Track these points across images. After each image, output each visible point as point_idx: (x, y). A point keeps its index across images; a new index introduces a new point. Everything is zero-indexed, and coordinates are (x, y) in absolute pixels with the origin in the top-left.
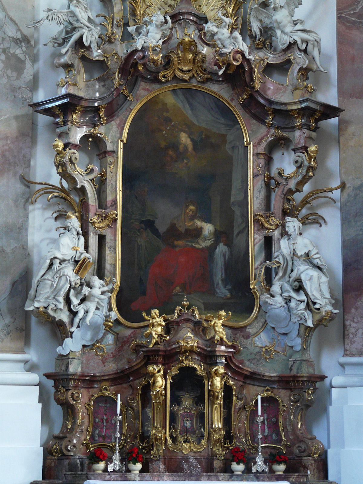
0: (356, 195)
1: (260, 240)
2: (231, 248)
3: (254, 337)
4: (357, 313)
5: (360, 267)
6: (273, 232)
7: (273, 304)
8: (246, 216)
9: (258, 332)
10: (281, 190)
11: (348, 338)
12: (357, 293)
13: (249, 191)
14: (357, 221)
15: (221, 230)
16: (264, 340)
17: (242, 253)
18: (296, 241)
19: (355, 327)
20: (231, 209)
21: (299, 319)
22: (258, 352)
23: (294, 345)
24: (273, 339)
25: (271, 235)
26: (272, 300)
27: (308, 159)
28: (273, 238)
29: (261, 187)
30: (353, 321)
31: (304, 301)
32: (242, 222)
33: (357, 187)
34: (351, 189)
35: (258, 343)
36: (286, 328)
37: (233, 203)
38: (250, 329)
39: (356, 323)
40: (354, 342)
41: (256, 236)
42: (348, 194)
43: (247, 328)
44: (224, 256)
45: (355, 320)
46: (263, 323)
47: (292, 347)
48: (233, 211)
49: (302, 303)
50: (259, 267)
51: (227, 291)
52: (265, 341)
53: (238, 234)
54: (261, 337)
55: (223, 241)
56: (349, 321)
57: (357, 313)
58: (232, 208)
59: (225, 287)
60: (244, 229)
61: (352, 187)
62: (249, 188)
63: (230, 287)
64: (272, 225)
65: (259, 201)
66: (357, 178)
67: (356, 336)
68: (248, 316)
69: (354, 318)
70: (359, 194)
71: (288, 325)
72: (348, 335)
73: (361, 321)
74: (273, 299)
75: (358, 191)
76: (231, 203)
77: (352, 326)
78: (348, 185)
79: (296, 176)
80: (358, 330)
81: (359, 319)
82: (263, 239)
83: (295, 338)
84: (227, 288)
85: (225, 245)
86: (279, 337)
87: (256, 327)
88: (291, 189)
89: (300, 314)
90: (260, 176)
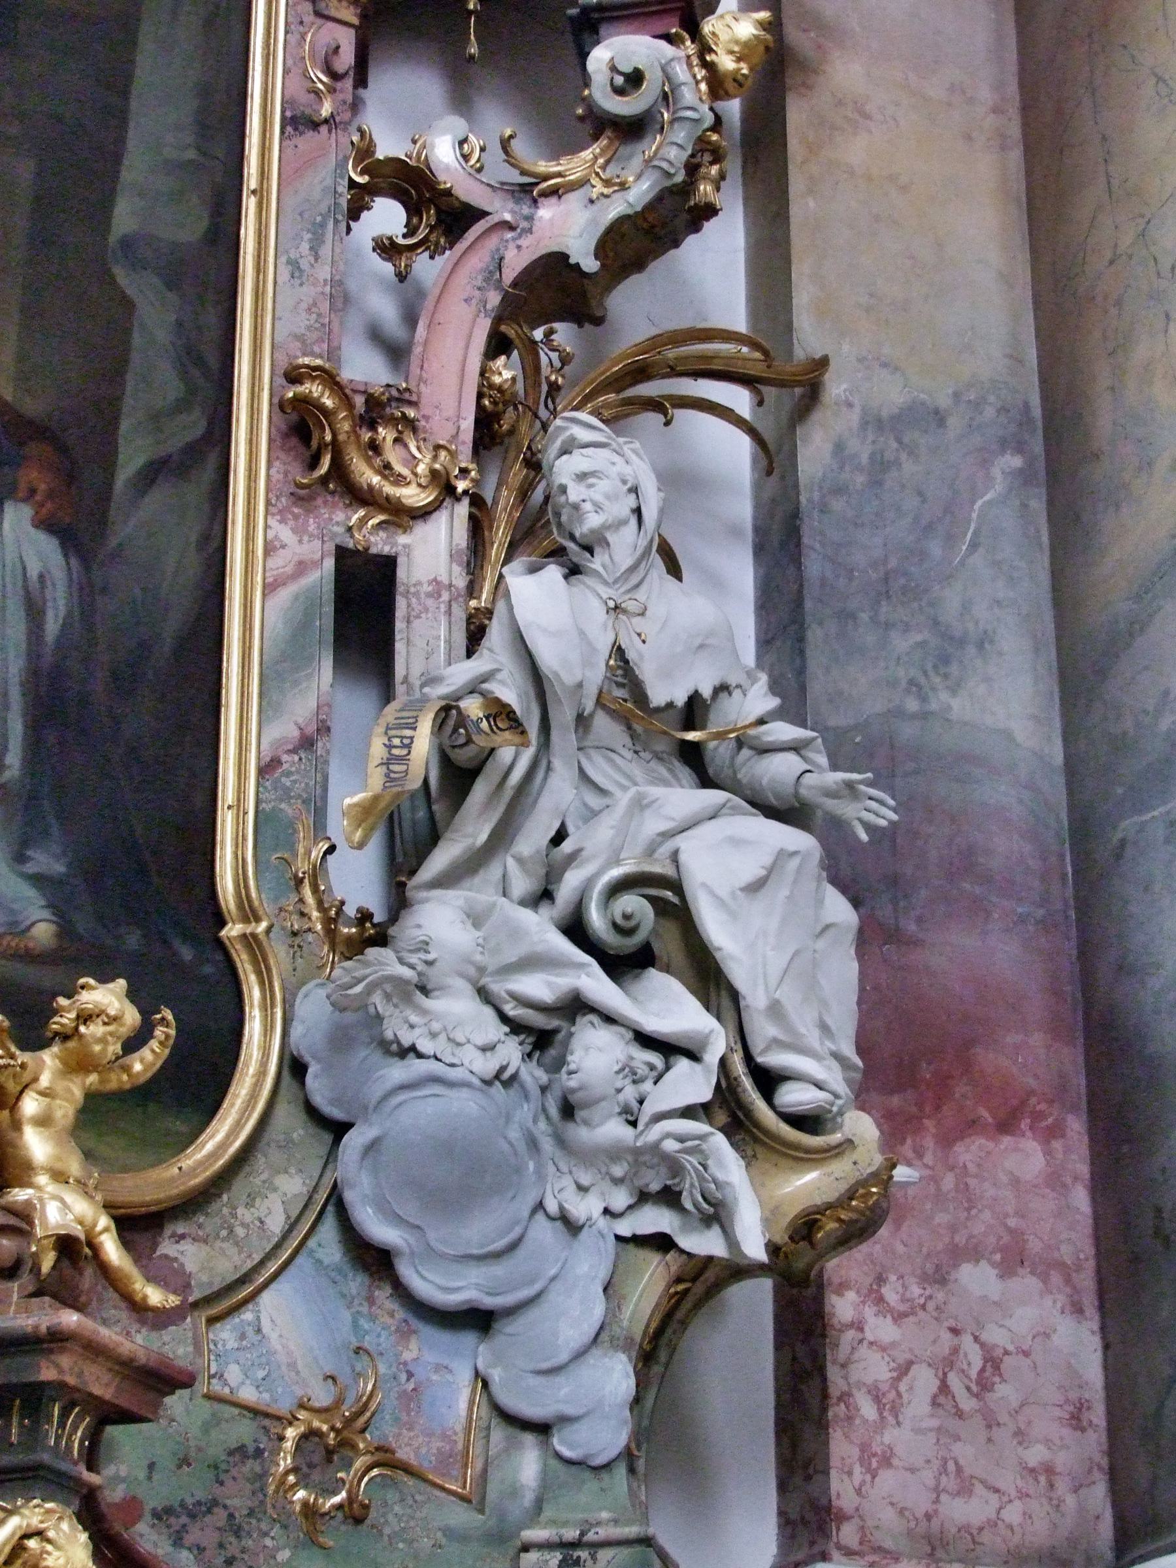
0: (880, 466)
1: (302, 568)
2: (86, 560)
3: (211, 1321)
4: (900, 1249)
5: (913, 927)
6: (406, 529)
7: (425, 1046)
8: (213, 362)
9: (243, 1280)
10: (479, 261)
11: (850, 1419)
12: (896, 1101)
13: (250, 205)
14: (888, 626)
15: (32, 407)
16: (282, 1358)
17: (172, 626)
18: (641, 595)
19: (894, 1345)
20: (113, 282)
21: (620, 1199)
22: (240, 1452)
23: (569, 1410)
24: (358, 1350)
25: (386, 550)
26: (414, 1018)
27: (703, 87)
28: (401, 573)
29: (323, 208)
30: (880, 1300)
31: (694, 1056)
32: (182, 406)
33: (885, 414)
34: (855, 417)
35: (233, 1374)
36: (498, 1270)
37: (127, 244)
38: (187, 1246)
39: (899, 1317)
40: (887, 1460)
41: (272, 522)
42: (839, 448)
43: (168, 1231)
44: (34, 612)
45: (890, 1293)
46: (294, 1214)
47: (543, 1429)
48: (128, 304)
49: (683, 1065)
50: (285, 758)
51: (30, 892)
52: (292, 1366)
53: (152, 474)
54: (259, 1331)
55: (33, 492)
56: (851, 1295)
57: (900, 1249)
58: (121, 276)
59: (20, 858)
60: (193, 453)
61: (857, 410)
62: (251, 179)
63: (59, 868)
64: (399, 480)
65: (307, 293)
66: (885, 365)
67: (895, 1411)
68: (180, 1126)
69: (881, 1280)
70: (897, 463)
71: (513, 1246)
72: (845, 1397)
73: (923, 1307)
74: (424, 1012)
75: (895, 445)
76: (113, 239)
77: (869, 1335)
78: (835, 387)
79: (607, 183)
80: (904, 1370)
81: (915, 1291)
82: (330, 564)
83: (580, 1355)
84: (30, 868)
85: (46, 524)
86: (414, 1344)
87: (240, 1232)
88: (564, 257)
89: (670, 1145)
90: (324, 129)
